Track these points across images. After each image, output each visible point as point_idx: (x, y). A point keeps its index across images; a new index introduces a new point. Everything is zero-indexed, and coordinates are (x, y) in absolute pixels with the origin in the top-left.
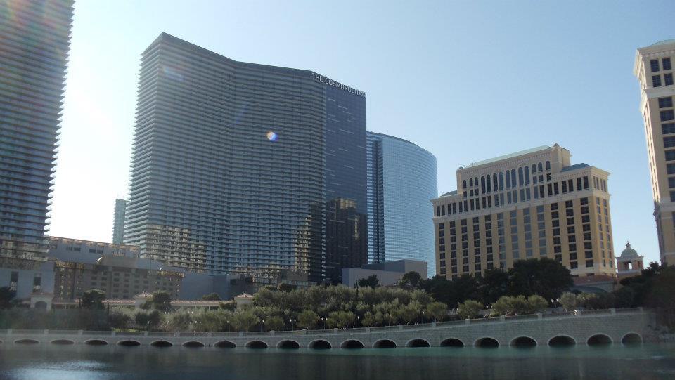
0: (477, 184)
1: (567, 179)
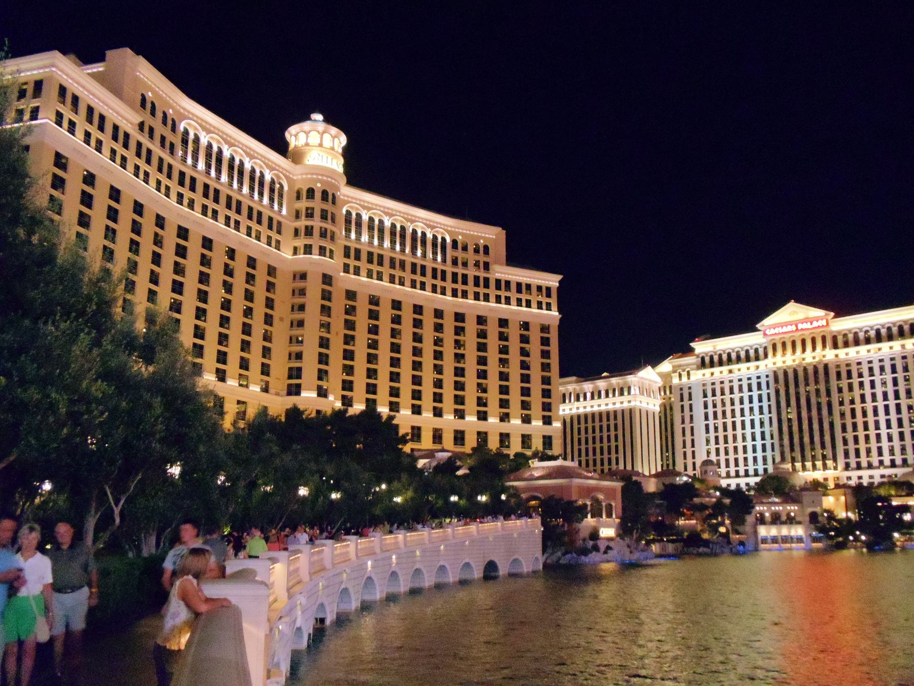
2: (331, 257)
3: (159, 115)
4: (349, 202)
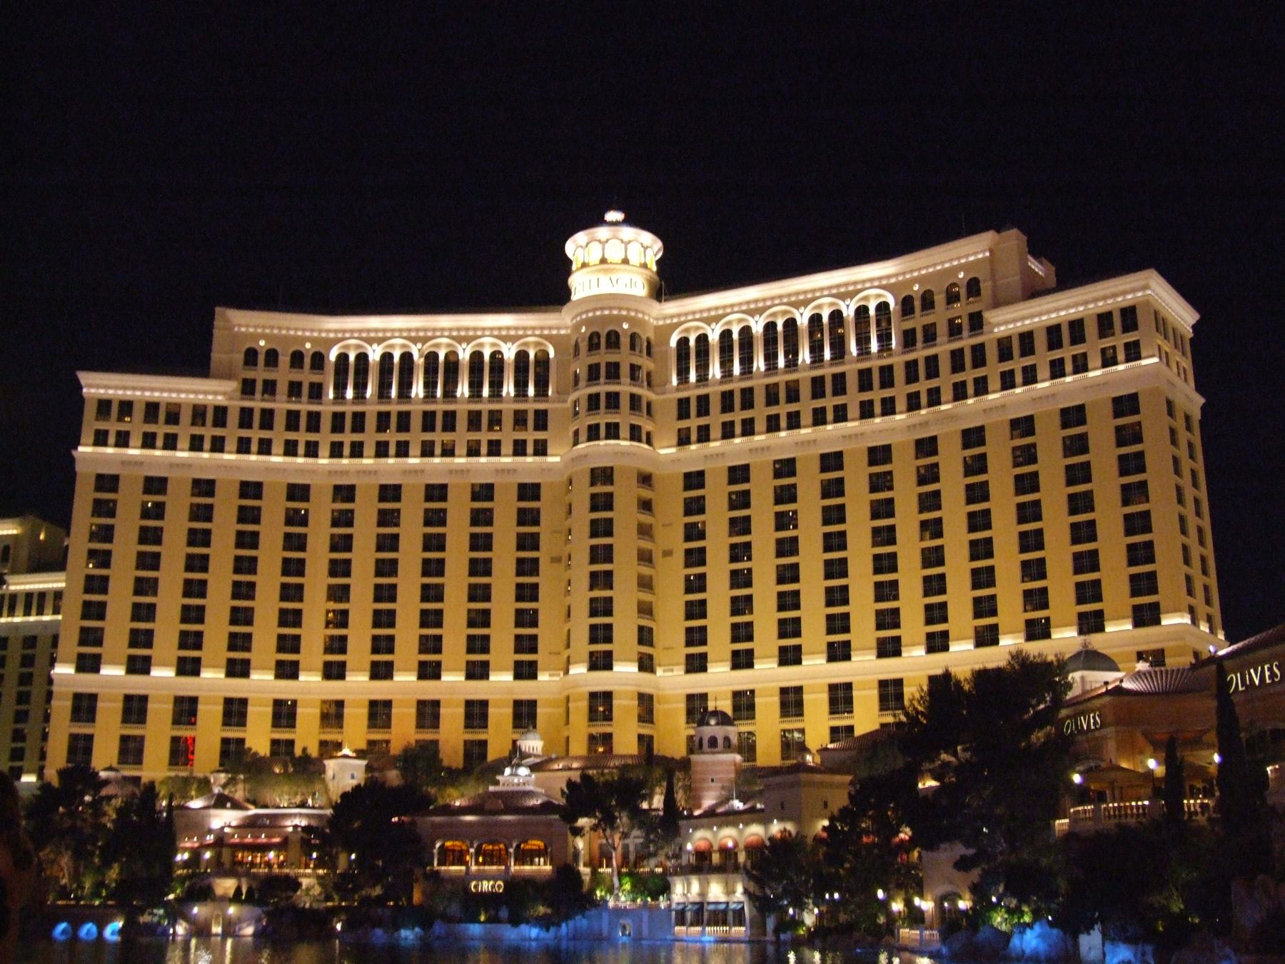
2: (613, 431)
3: (284, 360)
4: (674, 327)
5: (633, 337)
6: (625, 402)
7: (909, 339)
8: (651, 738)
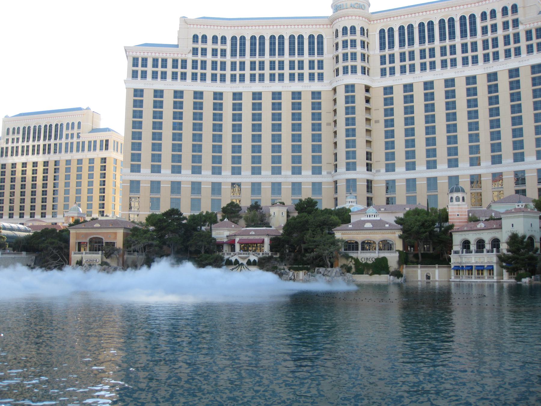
0: (18, 133)
1: (92, 140)
2: (354, 70)
5: (362, 29)
6: (359, 57)
7: (485, 30)
8: (371, 198)
